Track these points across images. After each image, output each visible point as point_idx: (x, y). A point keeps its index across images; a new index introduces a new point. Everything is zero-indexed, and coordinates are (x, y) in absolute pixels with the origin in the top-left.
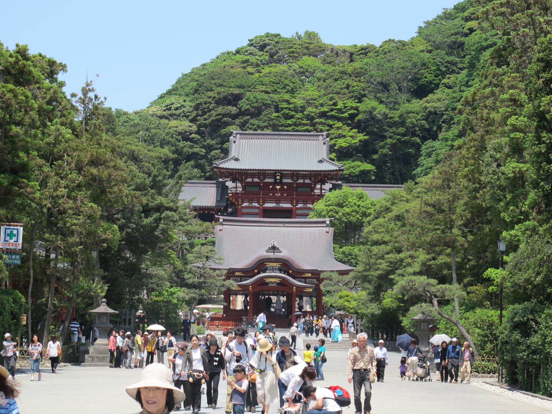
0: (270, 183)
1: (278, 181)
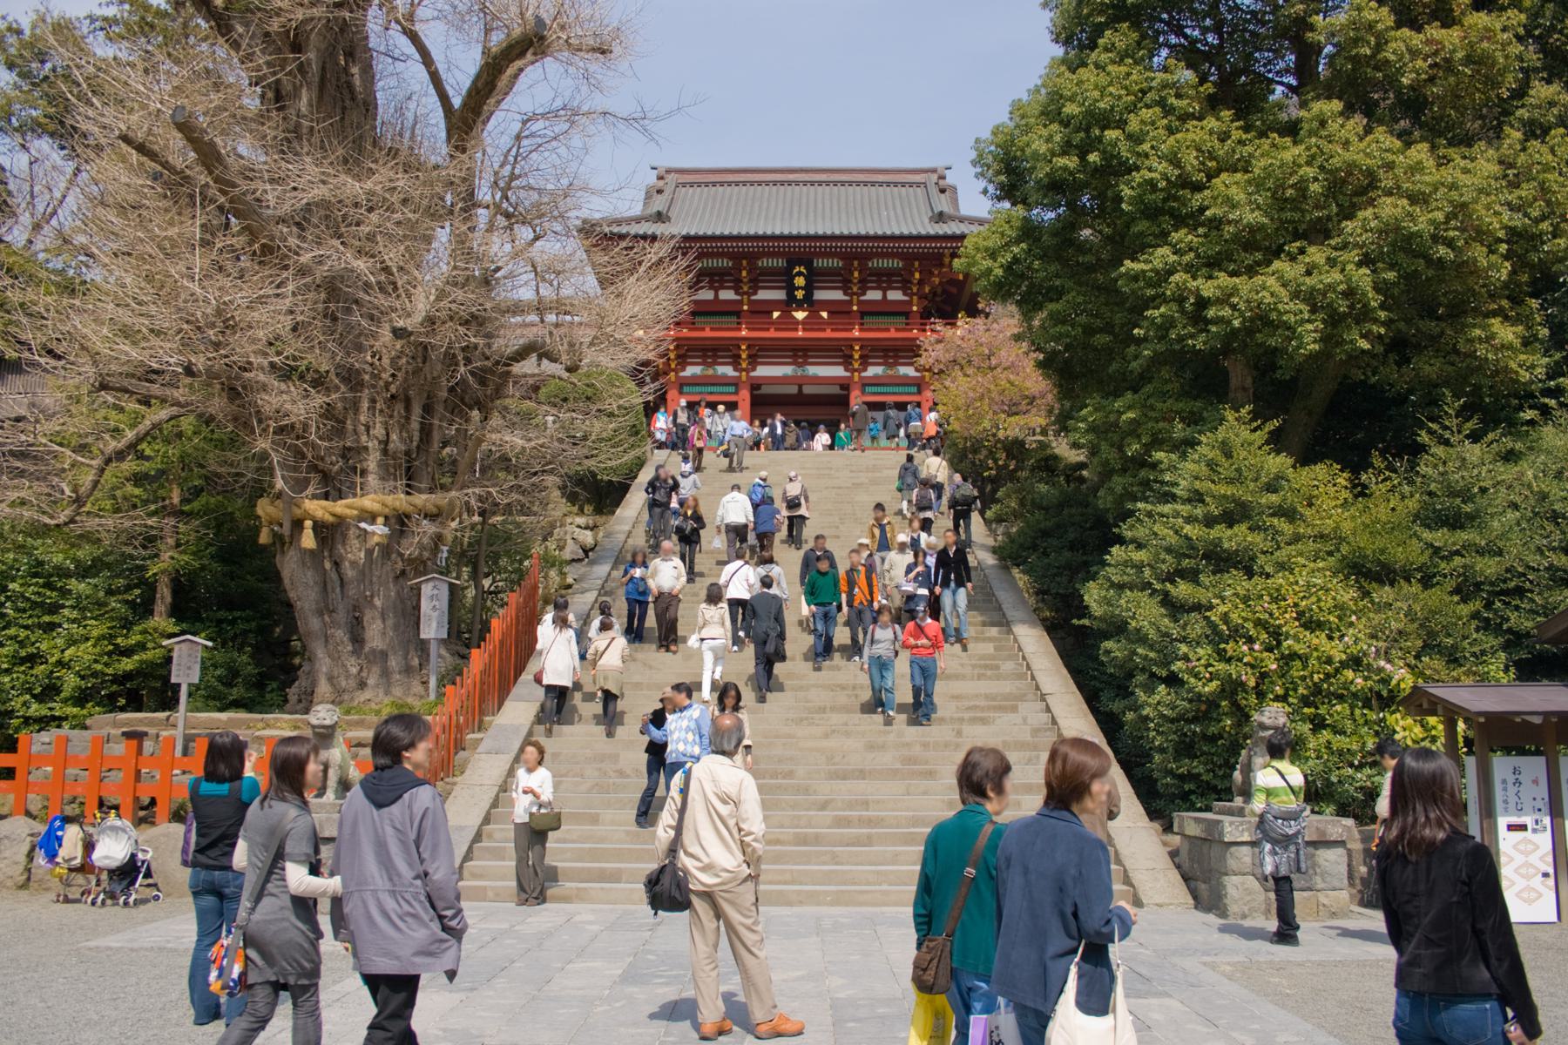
0: (775, 304)
1: (800, 294)
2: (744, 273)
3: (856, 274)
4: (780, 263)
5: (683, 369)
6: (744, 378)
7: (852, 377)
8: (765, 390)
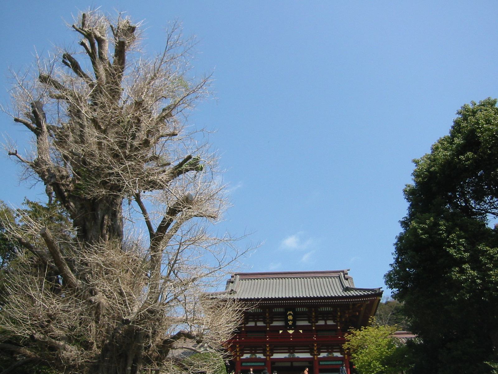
0: (280, 328)
1: (290, 323)
2: (267, 314)
3: (314, 314)
4: (281, 310)
5: (243, 356)
6: (268, 359)
7: (314, 358)
8: (277, 364)
